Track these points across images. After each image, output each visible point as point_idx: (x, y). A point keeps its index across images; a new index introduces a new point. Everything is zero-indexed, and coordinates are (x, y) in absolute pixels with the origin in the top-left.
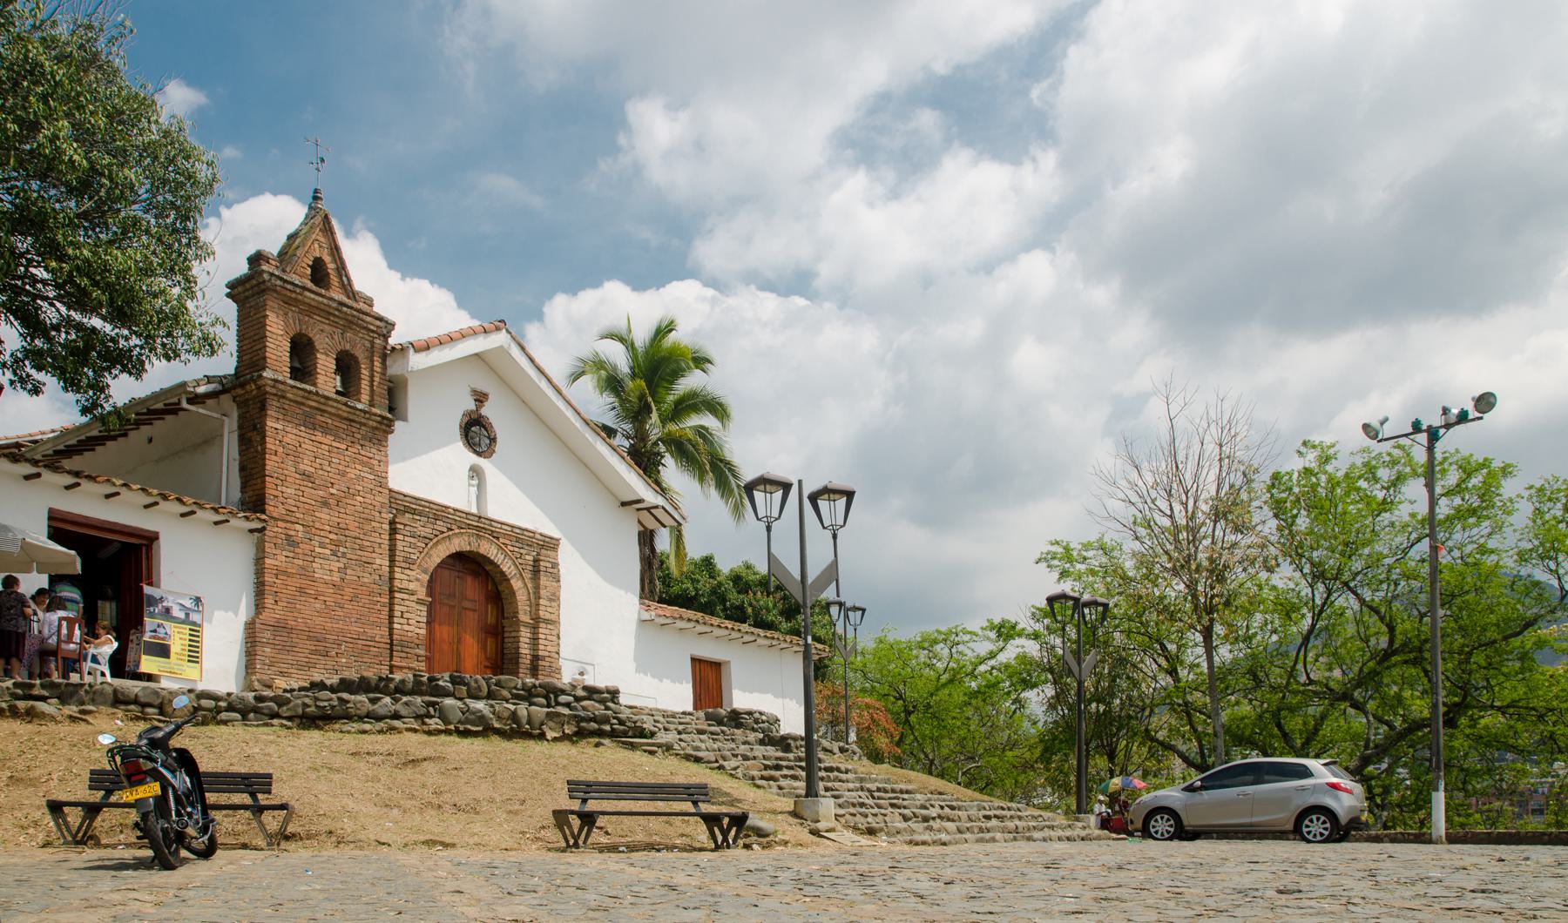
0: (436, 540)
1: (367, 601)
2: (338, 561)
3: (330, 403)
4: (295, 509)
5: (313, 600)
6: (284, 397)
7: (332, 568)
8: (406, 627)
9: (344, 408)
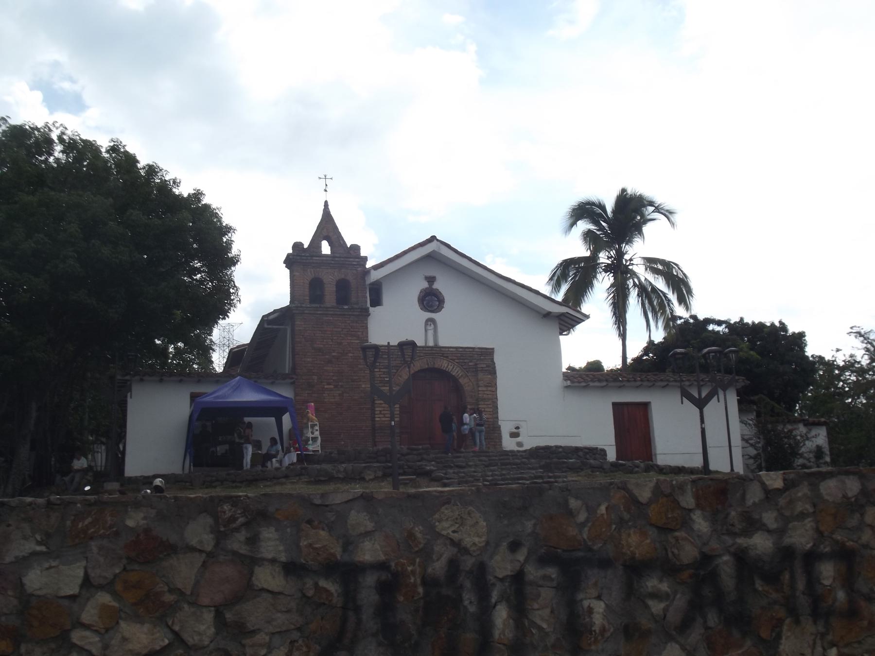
0: (403, 367)
4: (312, 368)
7: (335, 394)
8: (384, 419)
9: (338, 310)
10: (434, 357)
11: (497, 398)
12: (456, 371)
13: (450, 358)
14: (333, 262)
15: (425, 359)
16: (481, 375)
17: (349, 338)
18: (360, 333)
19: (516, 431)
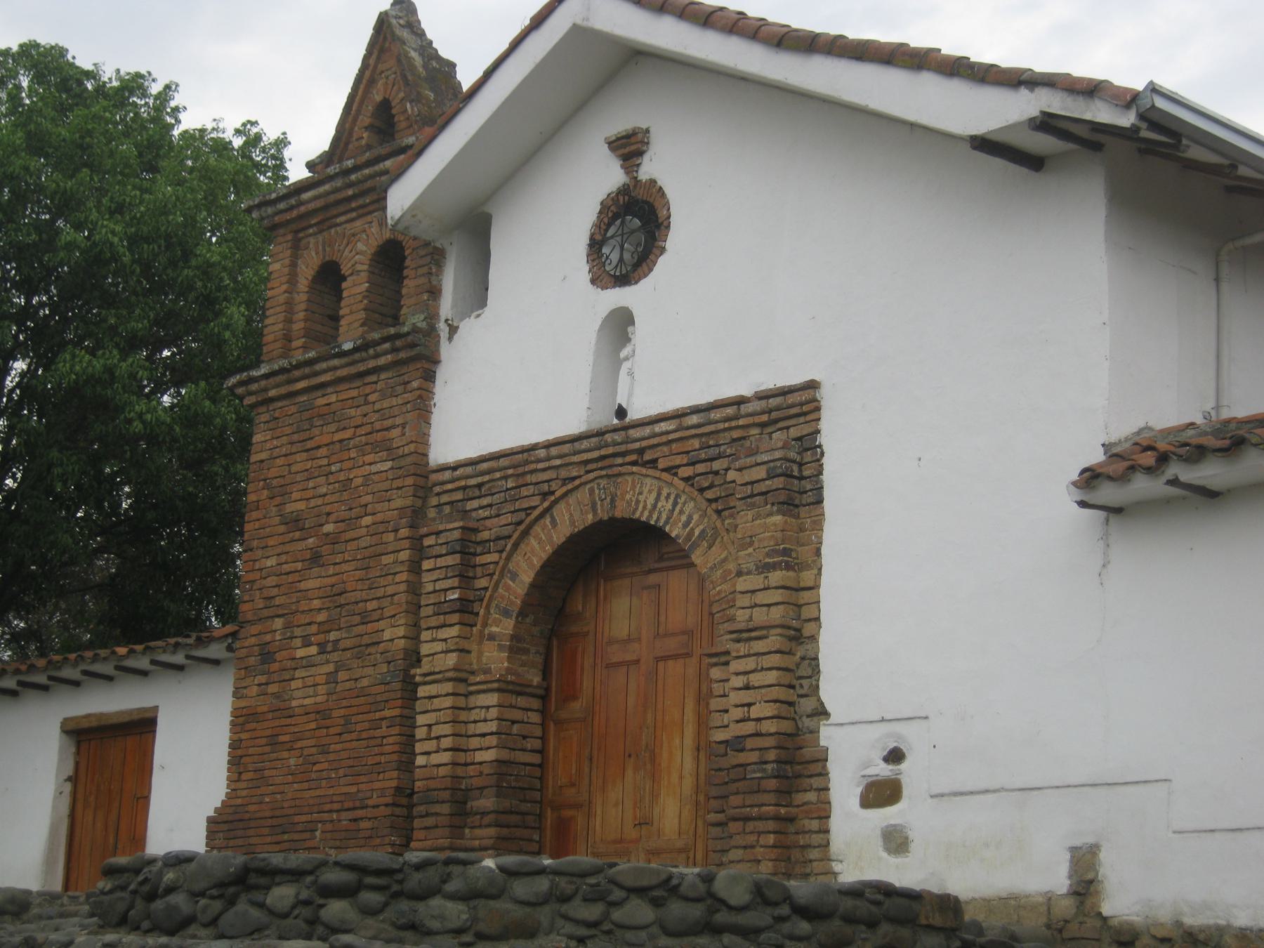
1: (367, 725)
2: (328, 662)
3: (318, 367)
5: (285, 754)
6: (272, 400)
8: (436, 759)
9: (336, 362)
10: (610, 472)
11: (818, 619)
12: (684, 518)
13: (662, 464)
14: (350, 192)
15: (588, 486)
16: (746, 520)
17: (368, 458)
18: (395, 433)
19: (883, 770)
